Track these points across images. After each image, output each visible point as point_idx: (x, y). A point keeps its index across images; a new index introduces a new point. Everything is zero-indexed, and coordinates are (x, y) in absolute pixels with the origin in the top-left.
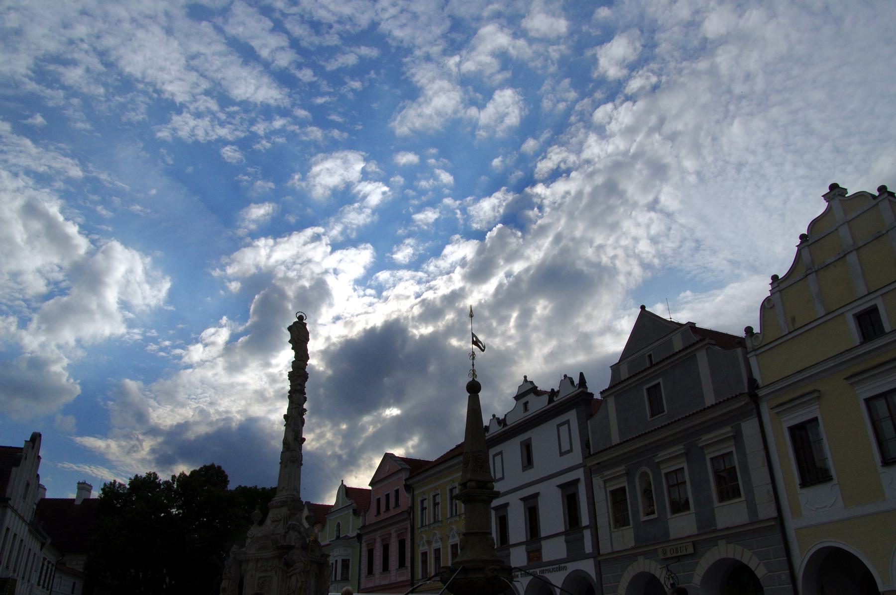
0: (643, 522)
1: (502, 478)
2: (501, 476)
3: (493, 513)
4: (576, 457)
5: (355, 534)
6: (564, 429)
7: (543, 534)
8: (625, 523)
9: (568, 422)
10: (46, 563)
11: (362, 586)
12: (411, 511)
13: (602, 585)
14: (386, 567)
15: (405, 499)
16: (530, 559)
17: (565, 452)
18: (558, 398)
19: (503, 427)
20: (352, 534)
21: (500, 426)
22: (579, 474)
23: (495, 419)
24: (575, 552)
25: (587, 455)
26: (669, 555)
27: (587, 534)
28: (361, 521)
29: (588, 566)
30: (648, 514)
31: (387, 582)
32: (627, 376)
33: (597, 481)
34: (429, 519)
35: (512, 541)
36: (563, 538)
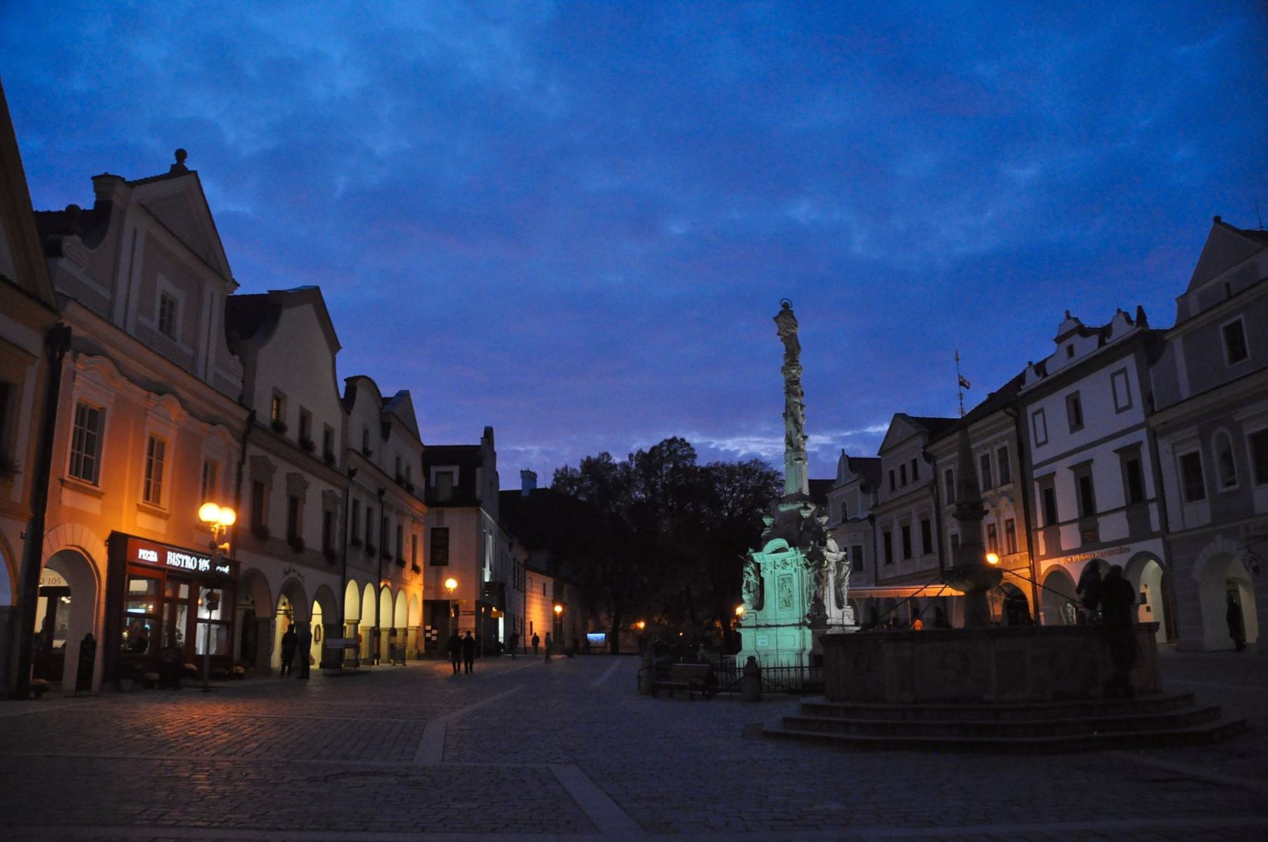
1: (1046, 442)
2: (1044, 440)
3: (1036, 484)
4: (1137, 414)
5: (866, 515)
7: (1099, 509)
11: (881, 576)
14: (908, 554)
15: (925, 469)
16: (1084, 541)
17: (1122, 409)
19: (1043, 377)
20: (863, 515)
21: (1039, 376)
22: (1141, 435)
23: (1032, 367)
24: (1139, 530)
25: (1150, 412)
27: (1154, 509)
28: (871, 499)
31: (911, 571)
32: (1198, 311)
33: (1163, 445)
35: (1062, 517)
36: (1124, 513)
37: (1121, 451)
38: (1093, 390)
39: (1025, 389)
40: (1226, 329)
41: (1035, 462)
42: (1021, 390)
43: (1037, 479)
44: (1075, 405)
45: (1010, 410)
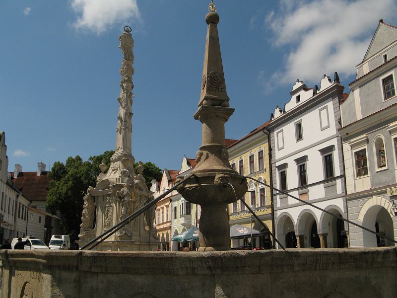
0: (377, 172)
1: (283, 148)
4: (333, 131)
6: (324, 112)
7: (309, 182)
8: (366, 173)
9: (326, 107)
10: (21, 206)
13: (348, 214)
18: (320, 91)
22: (334, 142)
29: (339, 203)
30: (381, 167)
35: (289, 187)
36: (322, 185)
37: (323, 151)
38: (309, 120)
40: (384, 81)
41: (277, 158)
43: (276, 167)
44: (299, 127)
45: (265, 131)
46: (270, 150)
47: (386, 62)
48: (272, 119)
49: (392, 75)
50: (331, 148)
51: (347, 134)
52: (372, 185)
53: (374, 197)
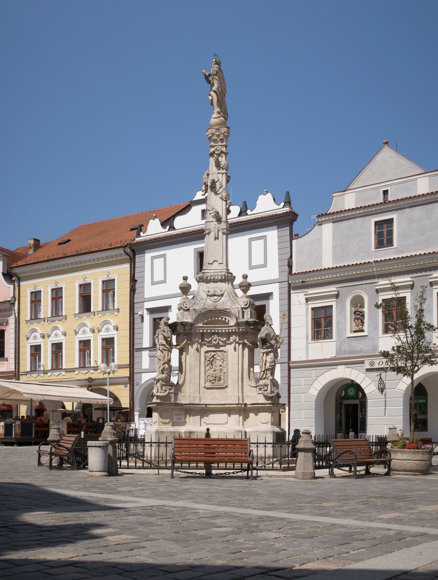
0: (348, 338)
1: (164, 281)
2: (162, 279)
12: (15, 301)
18: (254, 212)
19: (169, 230)
22: (274, 289)
26: (376, 366)
30: (355, 332)
34: (46, 312)
39: (143, 236)
41: (147, 295)
42: (140, 236)
45: (128, 250)
46: (133, 280)
47: (386, 202)
48: (142, 234)
49: (392, 219)
50: (267, 296)
51: (303, 282)
52: (337, 353)
53: (340, 367)
